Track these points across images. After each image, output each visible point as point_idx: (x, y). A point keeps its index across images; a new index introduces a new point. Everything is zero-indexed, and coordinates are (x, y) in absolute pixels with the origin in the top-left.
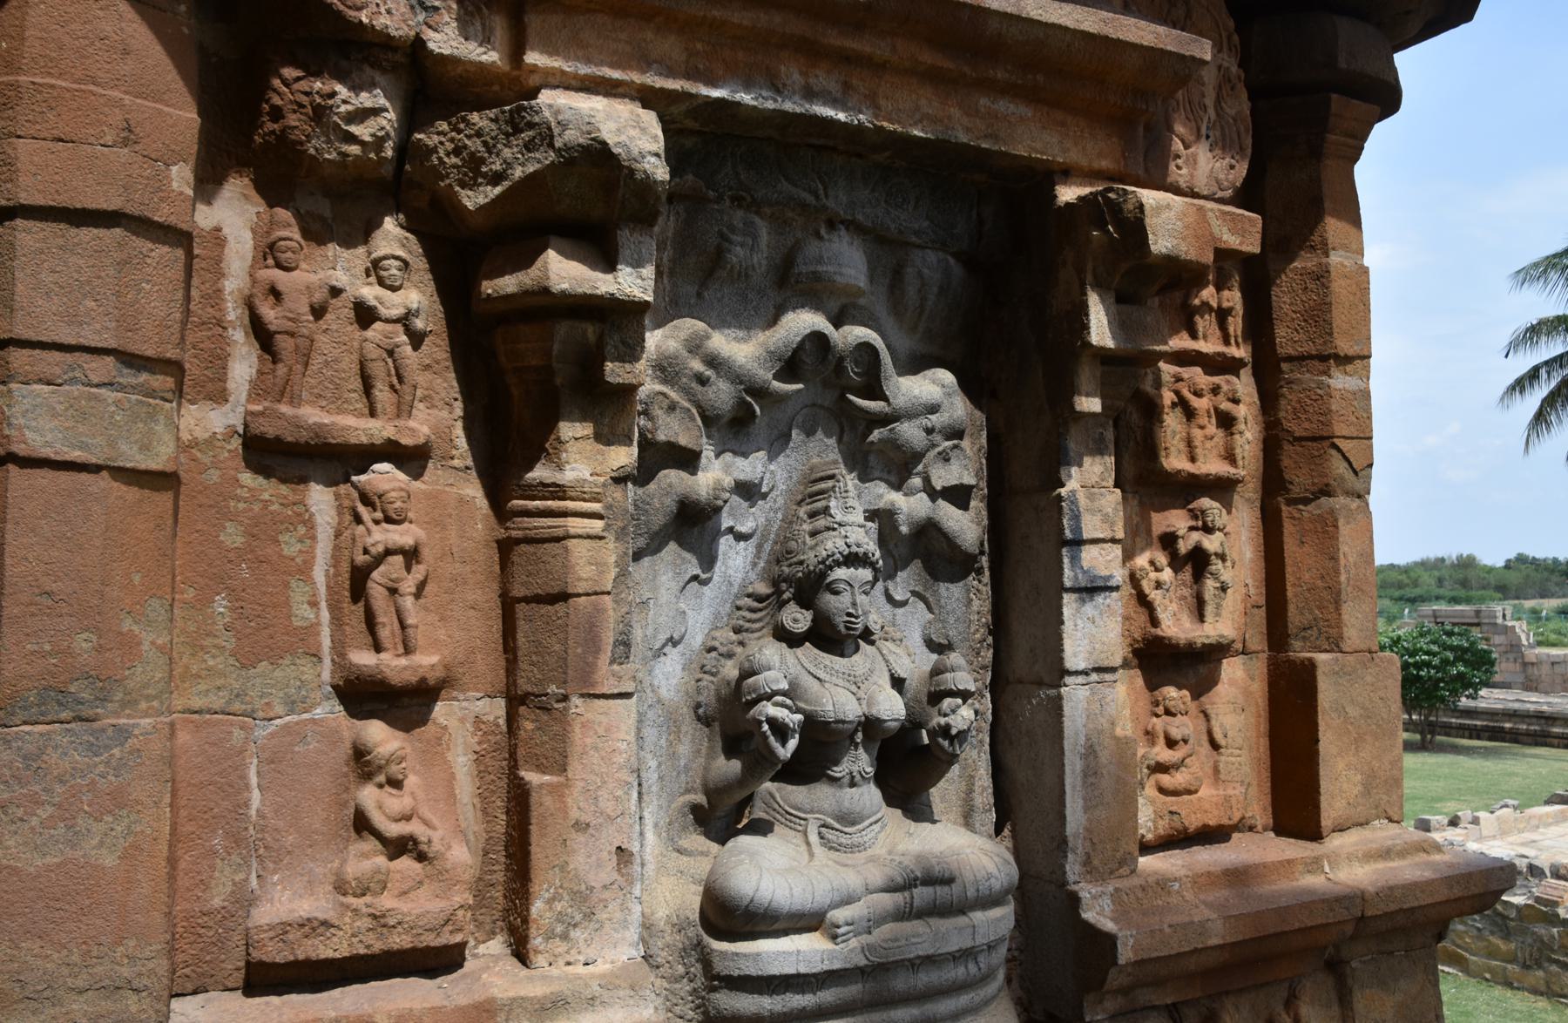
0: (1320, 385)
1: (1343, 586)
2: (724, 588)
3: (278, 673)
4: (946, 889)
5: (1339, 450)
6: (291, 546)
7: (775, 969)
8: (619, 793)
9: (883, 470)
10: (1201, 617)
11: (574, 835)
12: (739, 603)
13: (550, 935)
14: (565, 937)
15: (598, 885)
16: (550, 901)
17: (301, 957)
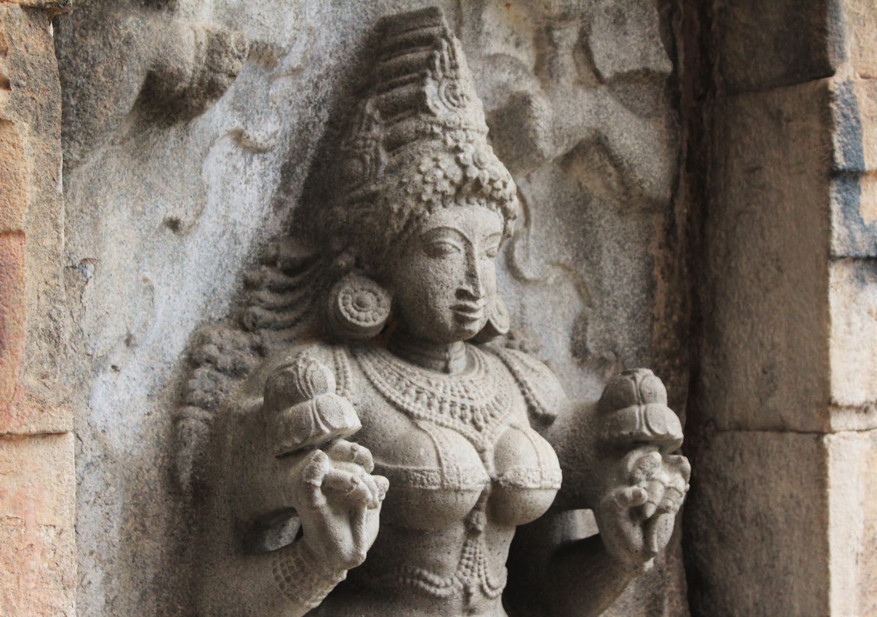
2: (223, 244)
9: (507, 40)
12: (254, 275)
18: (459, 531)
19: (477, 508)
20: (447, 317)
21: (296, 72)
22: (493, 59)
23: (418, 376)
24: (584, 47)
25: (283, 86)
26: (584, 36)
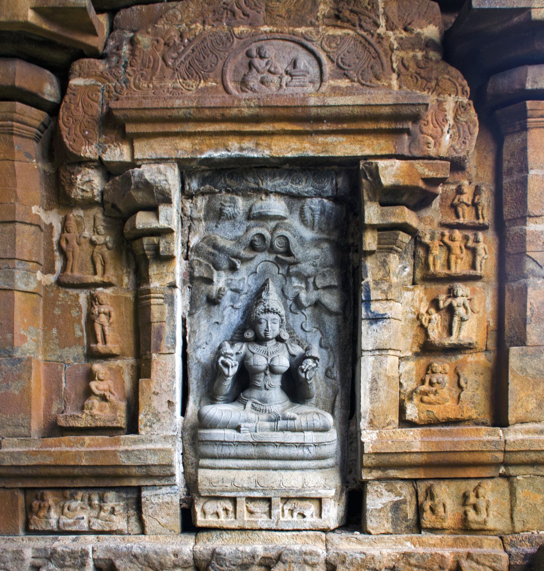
0: (521, 230)
1: (528, 317)
3: (71, 351)
4: (292, 422)
5: (530, 257)
6: (74, 313)
7: (217, 439)
8: (169, 384)
10: (450, 333)
11: (153, 396)
13: (145, 425)
14: (151, 426)
15: (161, 412)
16: (145, 415)
17: (71, 425)
18: (263, 374)
19: (266, 369)
20: (263, 335)
21: (246, 293)
22: (295, 287)
23: (258, 346)
24: (314, 283)
25: (244, 296)
26: (314, 279)
